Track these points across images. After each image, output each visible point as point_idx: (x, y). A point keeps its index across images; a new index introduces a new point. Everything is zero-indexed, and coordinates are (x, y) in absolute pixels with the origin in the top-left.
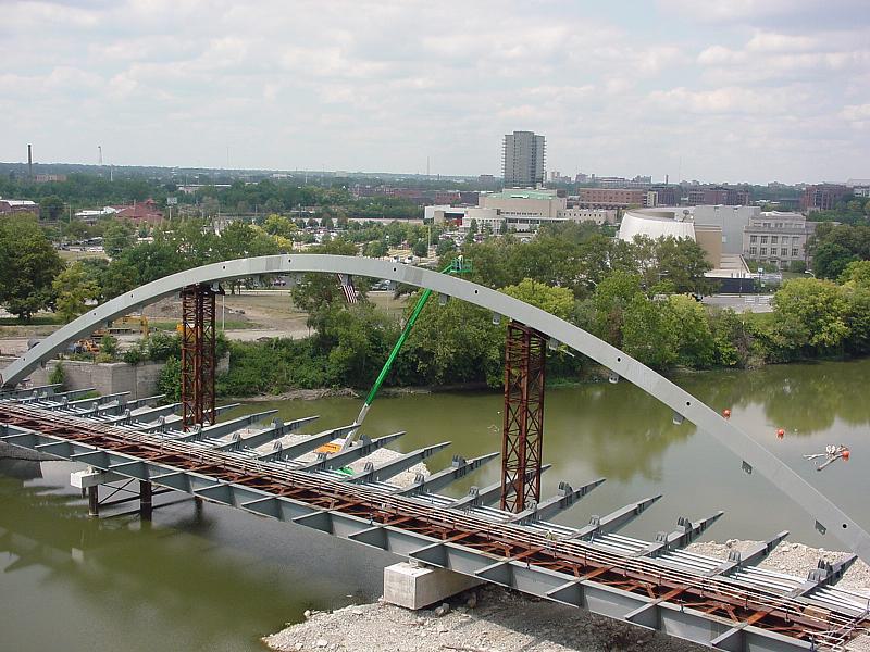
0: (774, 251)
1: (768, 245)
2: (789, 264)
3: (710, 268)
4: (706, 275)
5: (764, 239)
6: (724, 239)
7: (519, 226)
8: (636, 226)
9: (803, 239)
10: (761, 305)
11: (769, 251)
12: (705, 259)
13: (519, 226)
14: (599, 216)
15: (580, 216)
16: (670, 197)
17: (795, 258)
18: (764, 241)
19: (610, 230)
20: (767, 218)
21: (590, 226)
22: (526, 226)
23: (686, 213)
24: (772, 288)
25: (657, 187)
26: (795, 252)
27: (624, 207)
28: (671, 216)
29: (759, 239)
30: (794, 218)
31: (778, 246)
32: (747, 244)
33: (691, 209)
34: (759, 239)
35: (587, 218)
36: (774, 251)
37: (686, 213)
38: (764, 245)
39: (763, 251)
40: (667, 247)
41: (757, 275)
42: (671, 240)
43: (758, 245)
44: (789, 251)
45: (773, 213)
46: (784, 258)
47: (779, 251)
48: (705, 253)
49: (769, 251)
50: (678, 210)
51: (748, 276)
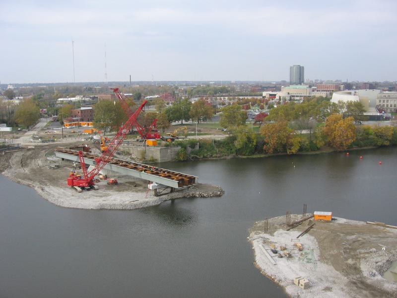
0: (387, 106)
3: (365, 111)
4: (364, 114)
5: (384, 102)
7: (296, 98)
8: (337, 98)
11: (386, 105)
12: (364, 108)
13: (296, 98)
14: (324, 94)
15: (318, 94)
16: (348, 87)
19: (328, 99)
20: (384, 93)
21: (321, 98)
22: (298, 98)
23: (355, 92)
24: (387, 119)
25: (344, 84)
28: (350, 93)
32: (378, 103)
33: (357, 91)
35: (321, 95)
36: (387, 106)
37: (355, 92)
39: (384, 105)
40: (350, 105)
41: (382, 114)
42: (351, 102)
43: (382, 103)
44: (393, 106)
45: (387, 92)
47: (389, 105)
48: (364, 106)
49: (386, 105)
50: (353, 92)
51: (378, 114)
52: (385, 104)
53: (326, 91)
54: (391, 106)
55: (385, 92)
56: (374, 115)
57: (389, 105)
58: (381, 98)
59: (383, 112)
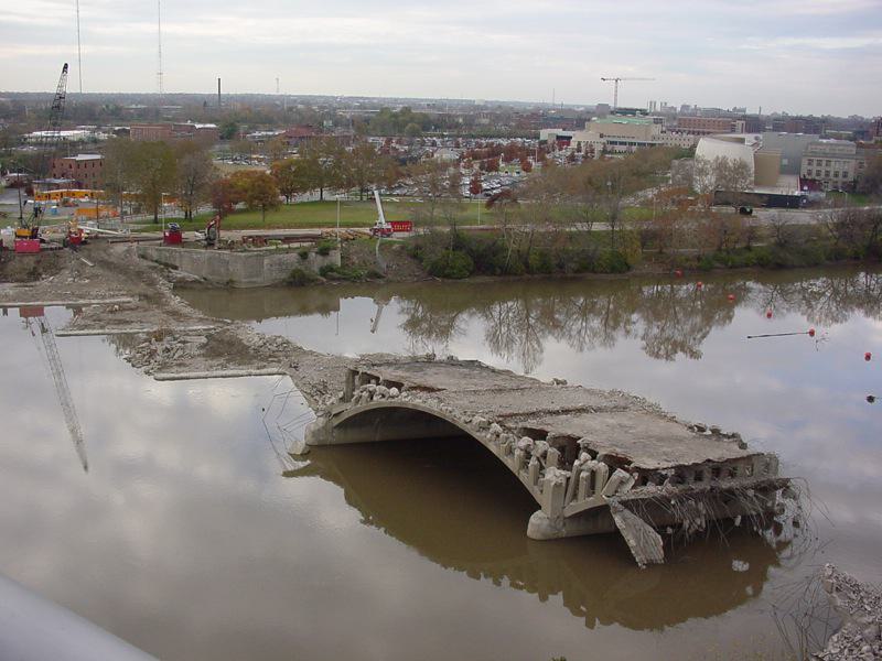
0: (827, 174)
1: (823, 169)
2: (840, 185)
5: (819, 164)
6: (785, 162)
7: (618, 148)
8: (709, 149)
9: (853, 163)
10: (802, 217)
13: (618, 148)
14: (684, 141)
15: (673, 140)
17: (845, 180)
18: (819, 164)
19: (691, 153)
20: (822, 144)
22: (623, 148)
23: (756, 138)
26: (845, 175)
27: (704, 133)
28: (742, 141)
29: (815, 163)
31: (835, 166)
33: (760, 136)
34: (815, 163)
35: (674, 142)
36: (827, 174)
38: (809, 168)
39: (818, 173)
43: (814, 168)
45: (832, 141)
46: (835, 179)
47: (832, 174)
49: (823, 174)
50: (750, 138)
52: (823, 169)
53: (693, 133)
54: (836, 175)
55: (825, 141)
56: (784, 194)
57: (832, 174)
58: (815, 154)
59: (806, 188)
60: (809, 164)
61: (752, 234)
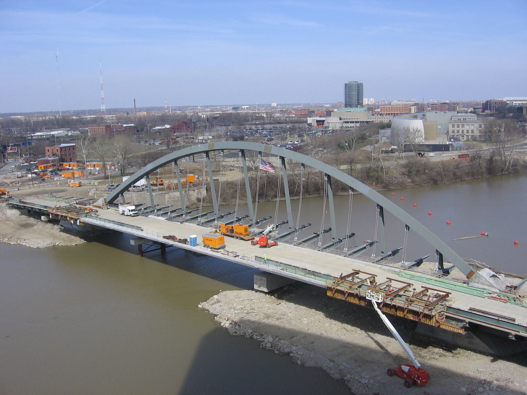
0: (463, 132)
1: (461, 129)
2: (470, 137)
5: (458, 127)
6: (439, 127)
9: (477, 125)
11: (461, 132)
14: (385, 120)
15: (377, 119)
17: (473, 134)
29: (456, 126)
30: (471, 116)
31: (466, 128)
34: (456, 126)
35: (381, 120)
39: (458, 132)
44: (470, 131)
47: (465, 131)
49: (461, 132)
50: (420, 115)
53: (389, 114)
54: (468, 132)
57: (465, 131)
60: (453, 127)
61: (427, 167)
